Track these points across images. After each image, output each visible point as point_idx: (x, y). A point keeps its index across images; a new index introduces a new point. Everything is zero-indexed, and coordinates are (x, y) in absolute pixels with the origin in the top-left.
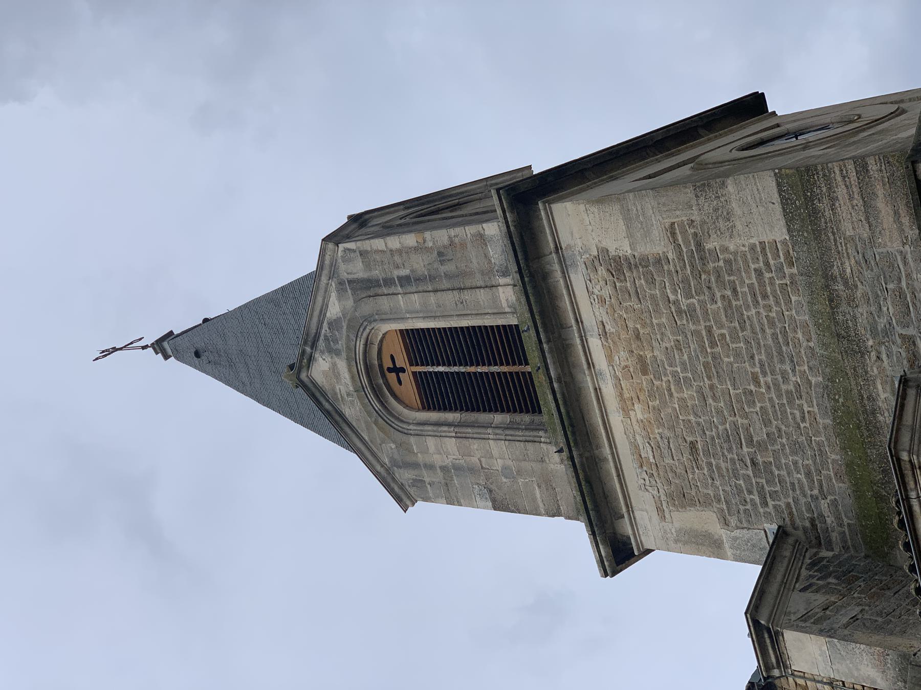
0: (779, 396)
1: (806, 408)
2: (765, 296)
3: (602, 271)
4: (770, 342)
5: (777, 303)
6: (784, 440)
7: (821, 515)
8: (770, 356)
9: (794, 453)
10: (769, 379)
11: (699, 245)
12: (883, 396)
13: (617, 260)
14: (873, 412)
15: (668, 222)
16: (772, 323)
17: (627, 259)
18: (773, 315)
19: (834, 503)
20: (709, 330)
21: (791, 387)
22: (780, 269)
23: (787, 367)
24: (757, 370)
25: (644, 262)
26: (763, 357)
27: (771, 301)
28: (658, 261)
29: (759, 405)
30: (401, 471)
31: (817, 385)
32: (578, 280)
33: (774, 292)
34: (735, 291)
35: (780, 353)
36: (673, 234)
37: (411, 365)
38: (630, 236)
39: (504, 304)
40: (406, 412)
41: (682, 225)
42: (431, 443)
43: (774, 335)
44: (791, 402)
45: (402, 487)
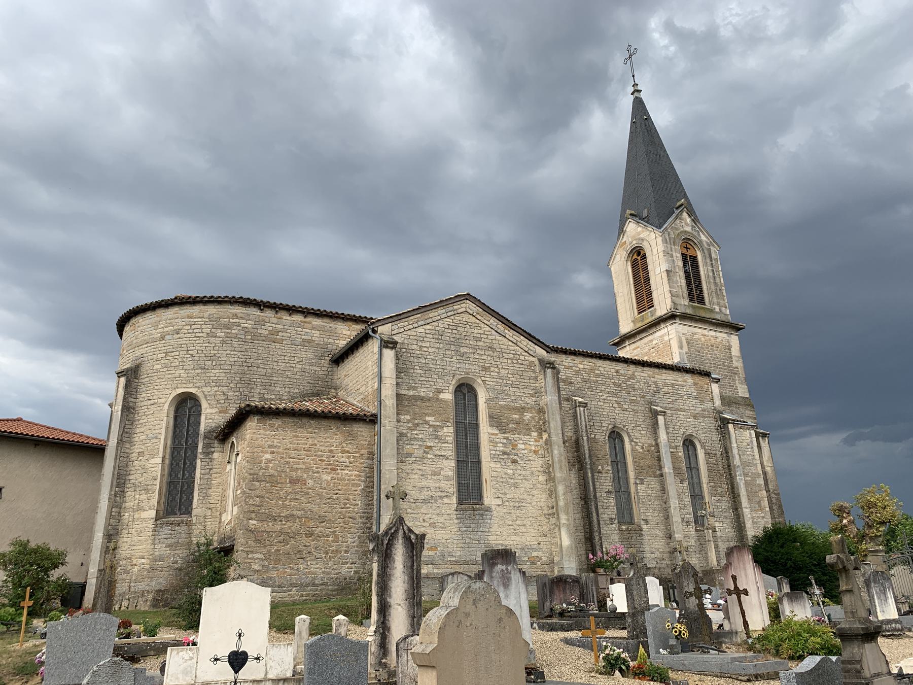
11: (736, 374)
13: (730, 350)
20: (722, 368)
22: (734, 392)
25: (731, 358)
28: (732, 361)
34: (730, 379)
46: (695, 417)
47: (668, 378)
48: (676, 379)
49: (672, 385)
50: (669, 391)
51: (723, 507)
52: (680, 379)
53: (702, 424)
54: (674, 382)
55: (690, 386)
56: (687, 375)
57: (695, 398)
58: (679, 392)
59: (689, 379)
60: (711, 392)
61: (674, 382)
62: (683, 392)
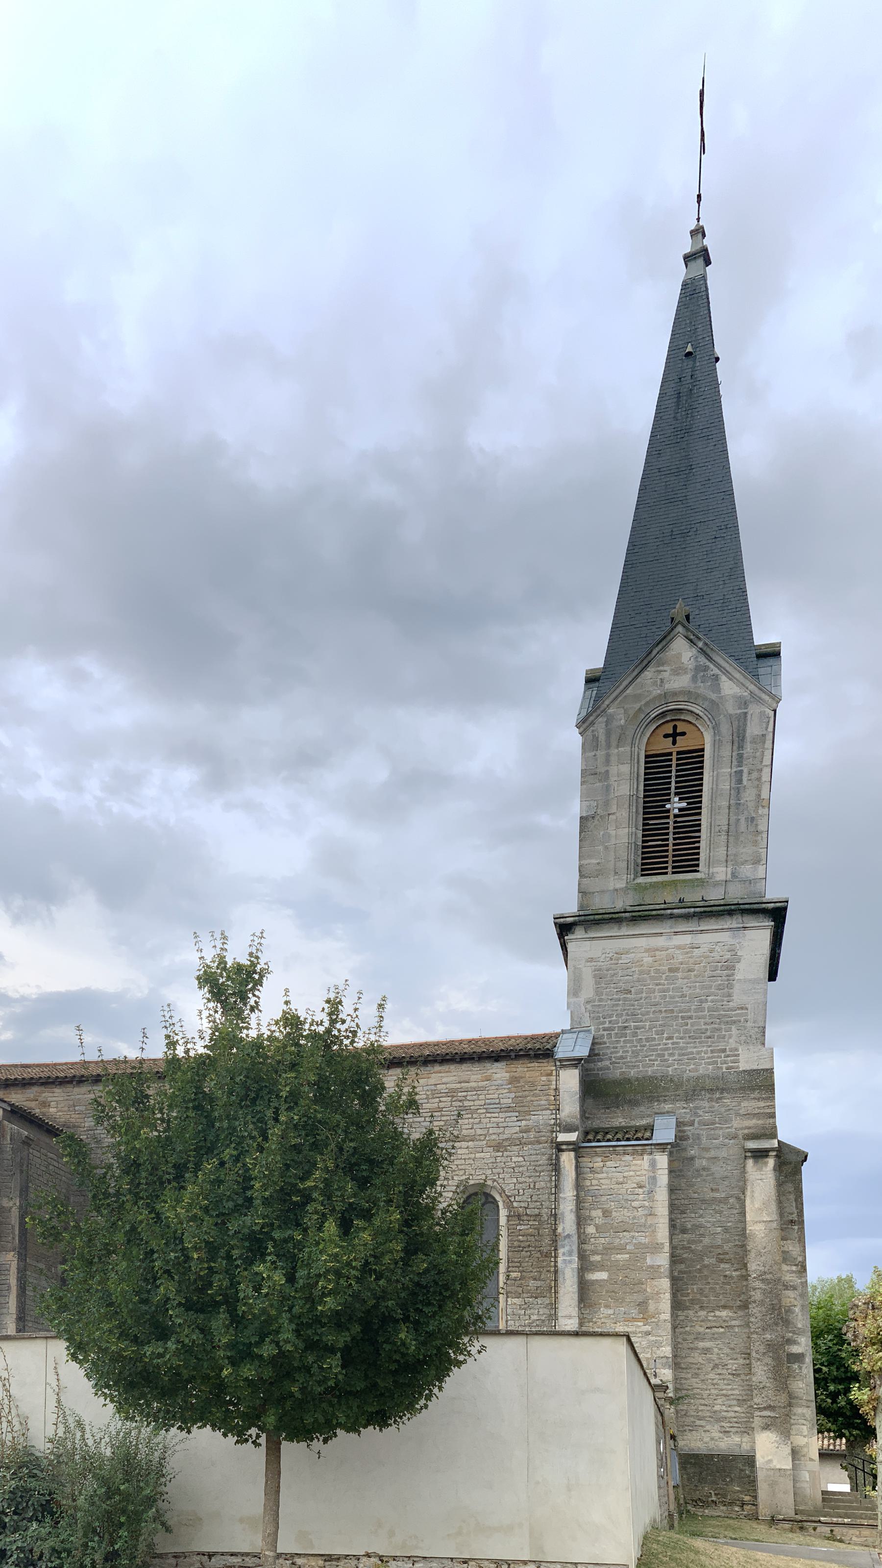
0: (661, 1050)
1: (656, 1063)
2: (712, 1052)
3: (728, 956)
4: (689, 1050)
5: (709, 1058)
6: (639, 1048)
7: (602, 1060)
8: (682, 1049)
9: (633, 1052)
10: (670, 1045)
12: (666, 1106)
14: (658, 1101)
15: (749, 1006)
16: (699, 1053)
17: (733, 974)
18: (703, 1055)
19: (609, 1069)
21: (666, 1057)
23: (676, 1057)
24: (675, 1040)
25: (730, 986)
26: (681, 1045)
27: (710, 1055)
29: (657, 1037)
30: (603, 725)
31: (668, 1071)
32: (725, 937)
33: (712, 1057)
35: (683, 1055)
36: (742, 1008)
37: (678, 753)
38: (745, 981)
39: (715, 870)
40: (645, 740)
41: (746, 1015)
42: (625, 769)
43: (692, 1053)
44: (658, 1055)
45: (592, 723)
46: (498, 1147)
47: (444, 1080)
48: (466, 1078)
49: (451, 1094)
50: (442, 1105)
51: (534, 1317)
52: (473, 1078)
53: (514, 1159)
54: (458, 1086)
55: (499, 1087)
56: (496, 1064)
57: (509, 1109)
58: (466, 1103)
59: (500, 1072)
60: (556, 1089)
61: (458, 1086)
62: (477, 1103)
